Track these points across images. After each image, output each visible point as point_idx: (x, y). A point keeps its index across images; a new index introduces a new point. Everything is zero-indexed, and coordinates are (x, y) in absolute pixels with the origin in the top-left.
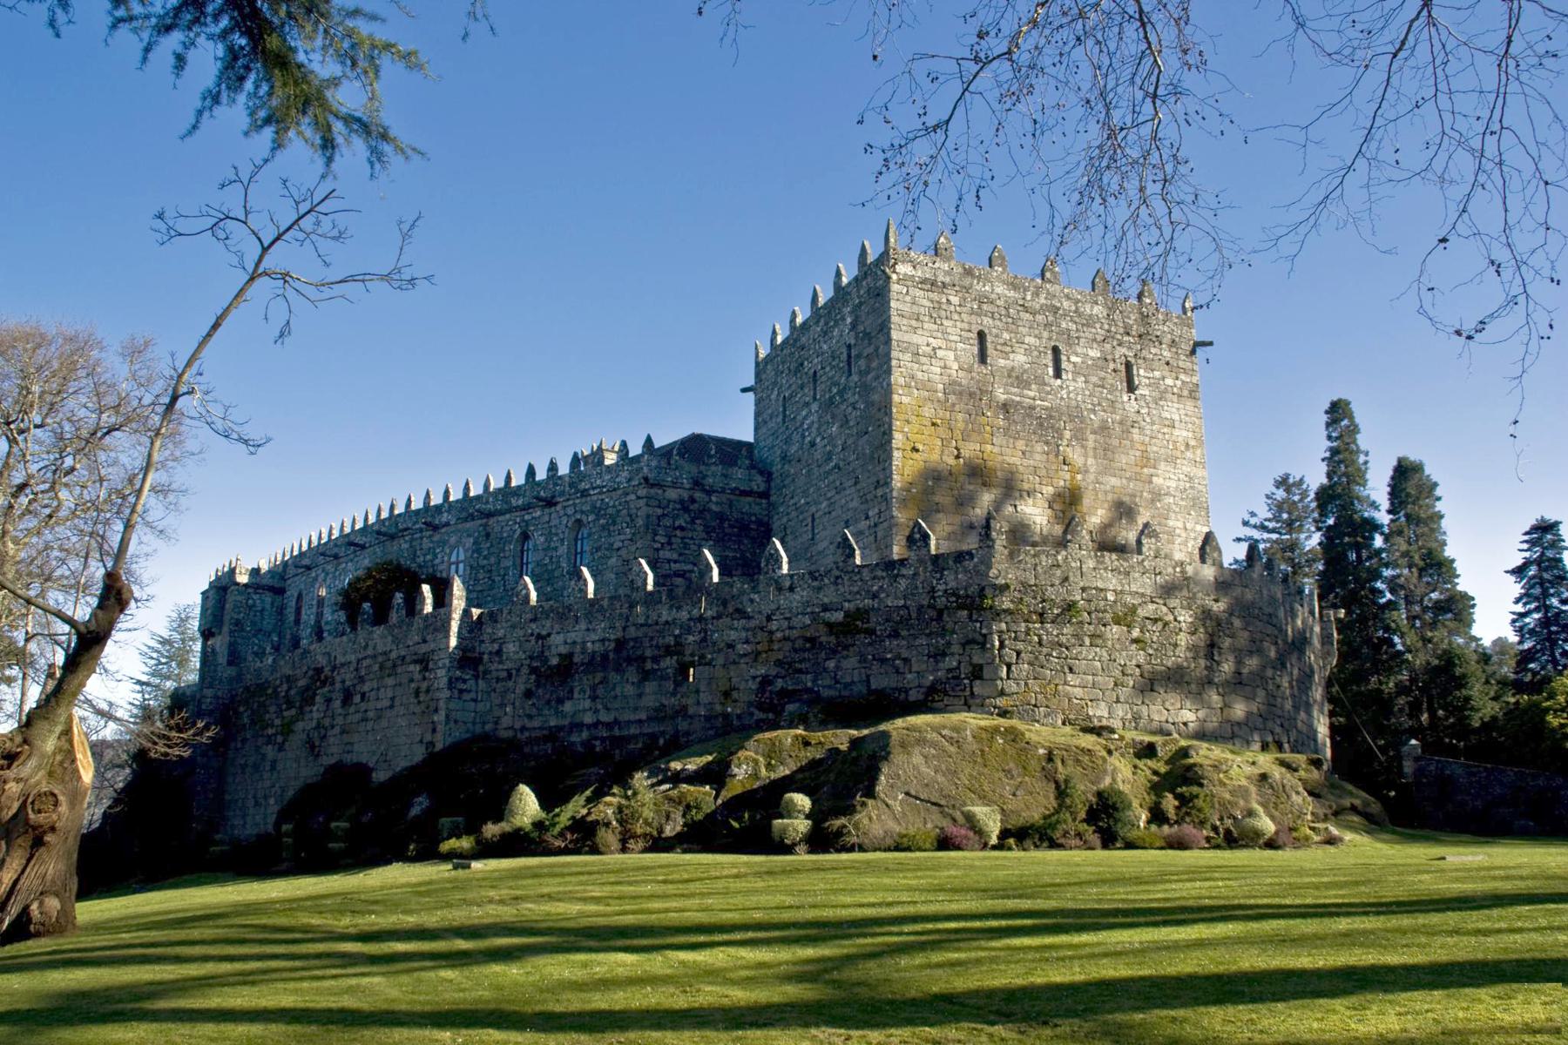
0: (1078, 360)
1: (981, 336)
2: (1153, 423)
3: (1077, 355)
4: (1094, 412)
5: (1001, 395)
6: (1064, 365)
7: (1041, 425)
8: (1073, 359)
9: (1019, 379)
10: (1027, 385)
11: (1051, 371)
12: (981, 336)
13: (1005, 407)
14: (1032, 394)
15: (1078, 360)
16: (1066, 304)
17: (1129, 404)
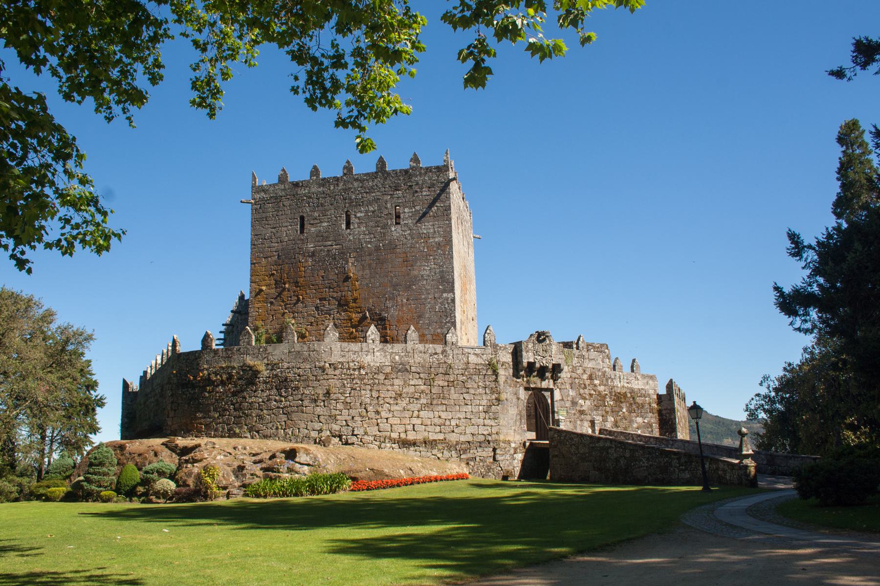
0: (362, 215)
1: (302, 218)
2: (413, 238)
3: (361, 212)
4: (370, 242)
5: (311, 246)
6: (353, 219)
7: (335, 259)
8: (359, 215)
9: (321, 237)
10: (326, 239)
11: (344, 226)
12: (302, 218)
13: (313, 255)
14: (330, 243)
15: (362, 215)
16: (356, 184)
17: (395, 231)
